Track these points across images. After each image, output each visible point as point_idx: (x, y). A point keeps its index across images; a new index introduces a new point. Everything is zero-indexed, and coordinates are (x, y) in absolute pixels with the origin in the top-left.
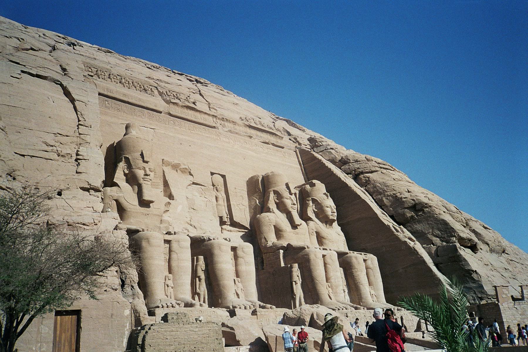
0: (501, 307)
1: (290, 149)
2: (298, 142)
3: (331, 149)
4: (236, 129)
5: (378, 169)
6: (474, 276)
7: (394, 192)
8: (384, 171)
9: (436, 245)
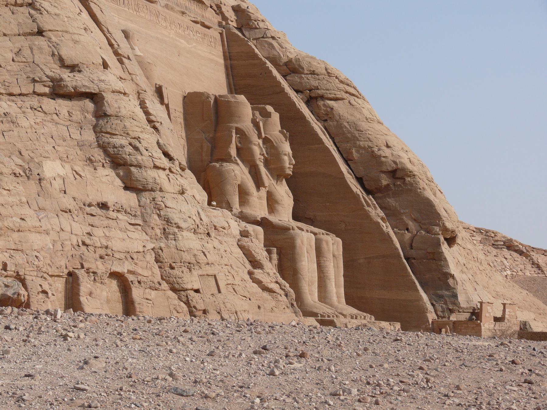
0: (483, 328)
1: (215, 30)
2: (222, 14)
6: (451, 281)
8: (352, 99)
9: (412, 233)
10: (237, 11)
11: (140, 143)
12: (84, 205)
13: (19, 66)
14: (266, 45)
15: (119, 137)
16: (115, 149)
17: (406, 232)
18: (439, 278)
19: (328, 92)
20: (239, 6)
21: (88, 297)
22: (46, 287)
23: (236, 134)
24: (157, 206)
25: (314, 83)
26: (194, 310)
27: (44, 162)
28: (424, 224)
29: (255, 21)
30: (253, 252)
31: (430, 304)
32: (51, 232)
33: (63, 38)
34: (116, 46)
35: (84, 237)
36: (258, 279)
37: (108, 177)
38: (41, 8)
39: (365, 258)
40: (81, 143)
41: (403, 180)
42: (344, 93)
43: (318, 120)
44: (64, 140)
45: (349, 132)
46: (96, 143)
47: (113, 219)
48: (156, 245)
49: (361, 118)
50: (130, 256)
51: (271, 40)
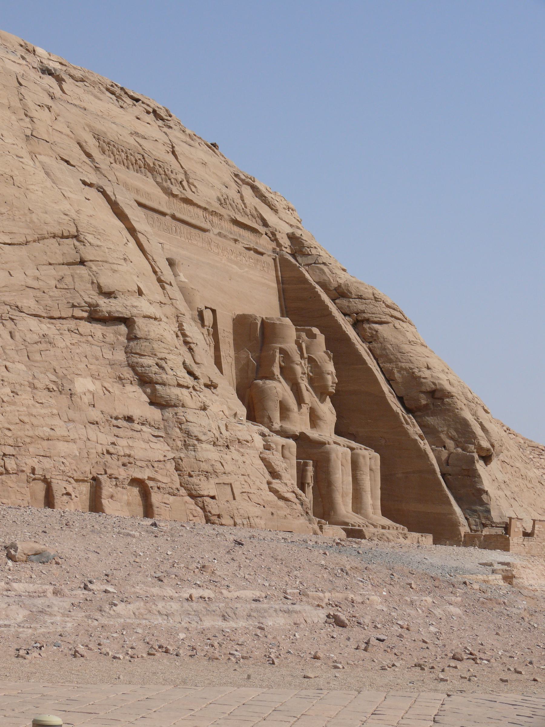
1: (269, 256)
2: (276, 240)
3: (324, 264)
4: (222, 228)
5: (389, 319)
6: (484, 497)
8: (397, 323)
9: (448, 450)
10: (292, 238)
11: (166, 363)
12: (111, 418)
13: (61, 292)
14: (317, 271)
15: (147, 357)
16: (143, 369)
17: (443, 449)
18: (473, 494)
19: (373, 315)
20: (293, 234)
21: (110, 500)
22: (70, 489)
24: (178, 420)
25: (361, 307)
26: (209, 514)
27: (75, 379)
28: (460, 442)
29: (308, 248)
30: (273, 464)
31: (463, 517)
32: (78, 441)
33: (102, 268)
34: (159, 273)
35: (108, 446)
37: (135, 393)
38: (84, 240)
39: (403, 473)
40: (112, 362)
41: (442, 400)
42: (389, 317)
43: (363, 342)
44: (97, 359)
46: (126, 363)
47: (137, 431)
48: (177, 455)
49: (404, 340)
50: (150, 463)
51: (322, 266)
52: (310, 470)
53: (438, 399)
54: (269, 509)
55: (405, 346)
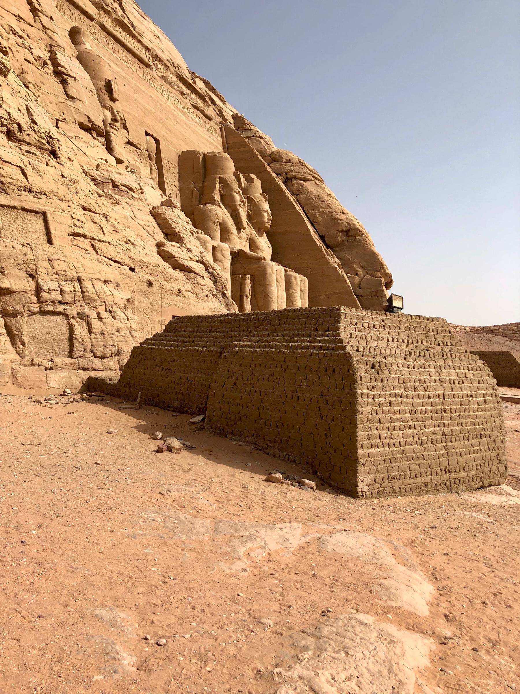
7: (330, 210)
8: (317, 182)
9: (360, 277)
23: (220, 183)
25: (290, 168)
28: (370, 270)
30: (170, 221)
36: (168, 252)
39: (325, 295)
45: (315, 202)
51: (259, 139)
52: (248, 282)
53: (351, 236)
54: (143, 275)
55: (325, 197)
